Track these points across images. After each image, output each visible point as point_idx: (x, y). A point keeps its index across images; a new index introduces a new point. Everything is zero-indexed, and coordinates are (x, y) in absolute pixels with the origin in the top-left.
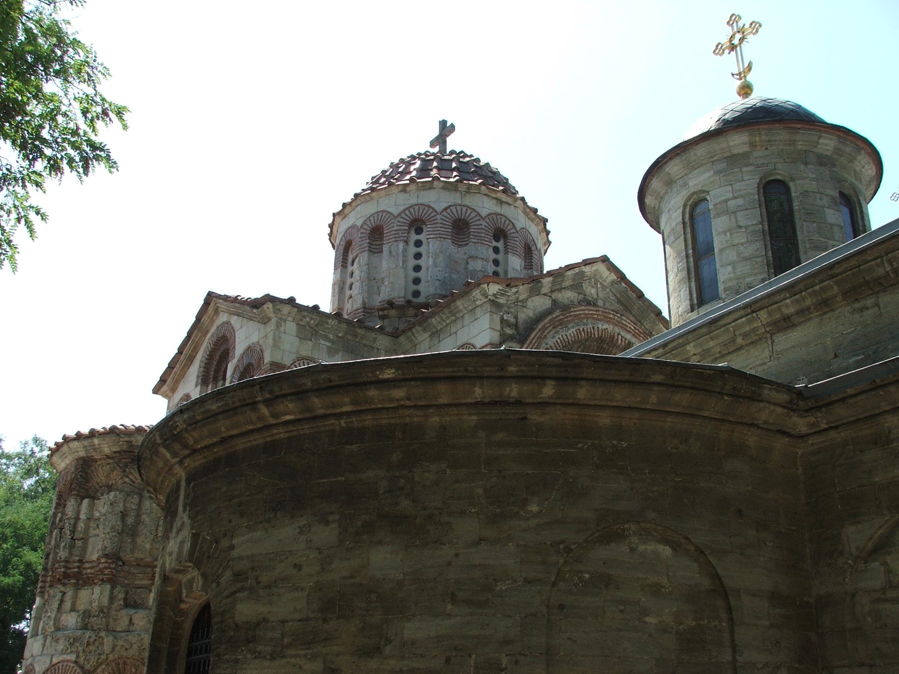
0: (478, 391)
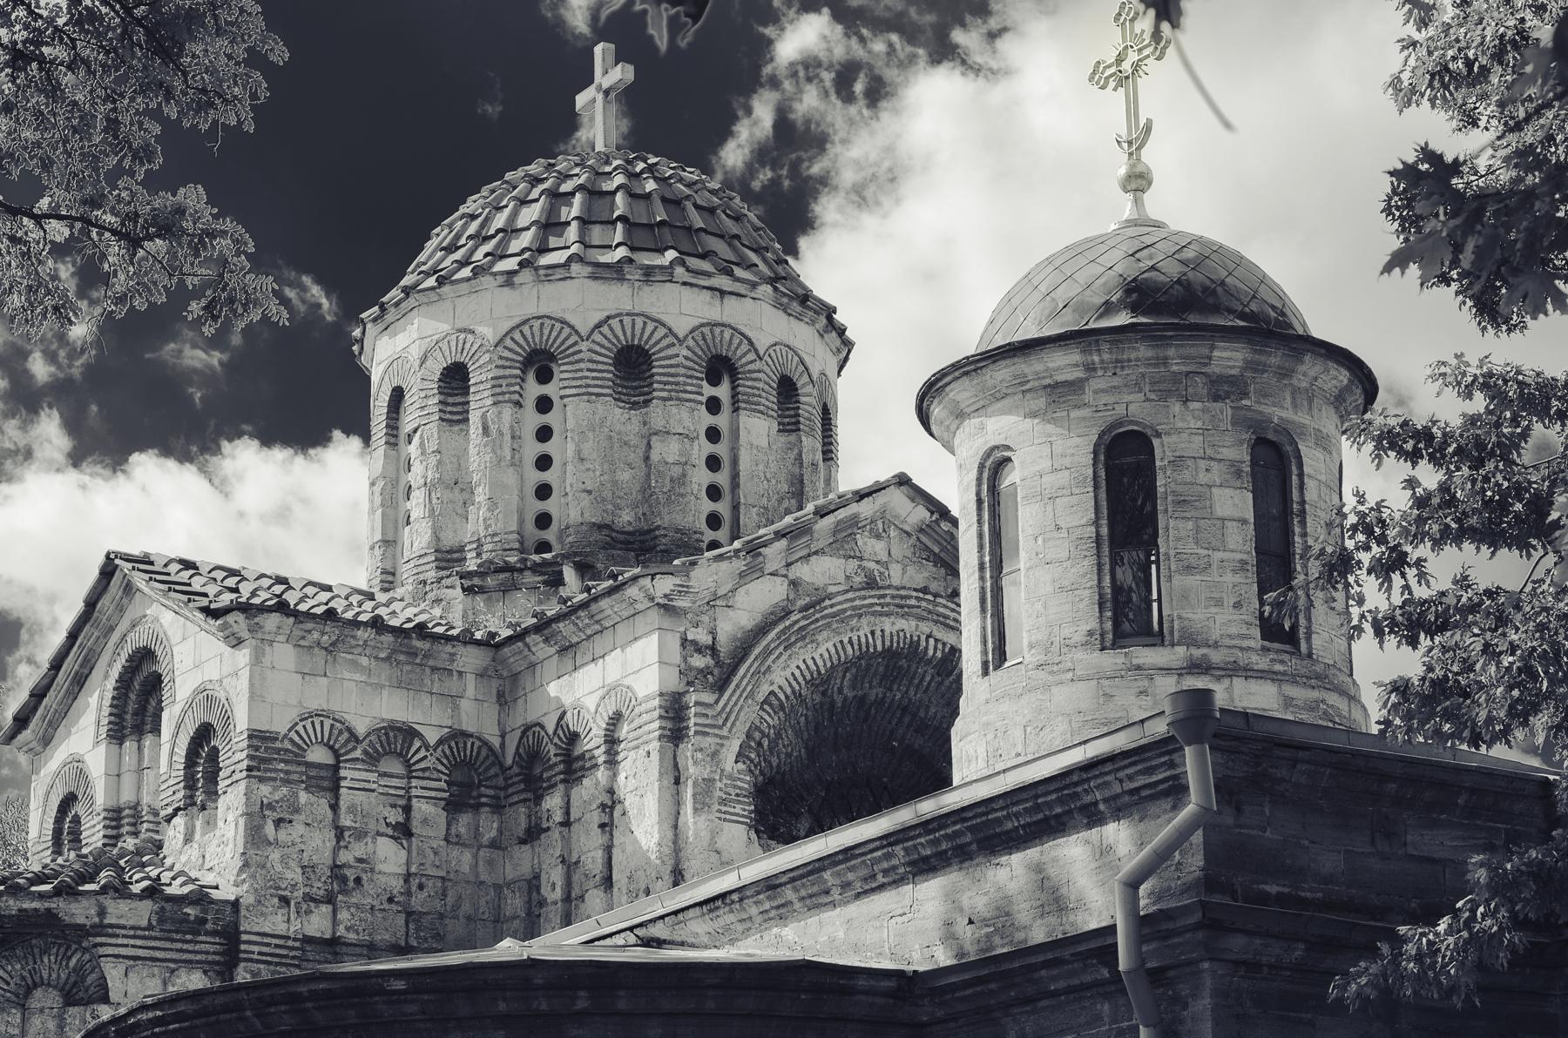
0: (502, 1006)
